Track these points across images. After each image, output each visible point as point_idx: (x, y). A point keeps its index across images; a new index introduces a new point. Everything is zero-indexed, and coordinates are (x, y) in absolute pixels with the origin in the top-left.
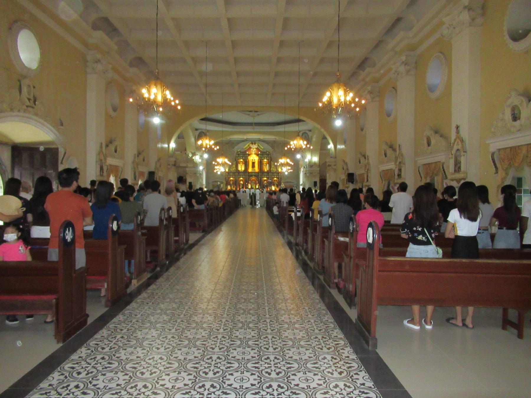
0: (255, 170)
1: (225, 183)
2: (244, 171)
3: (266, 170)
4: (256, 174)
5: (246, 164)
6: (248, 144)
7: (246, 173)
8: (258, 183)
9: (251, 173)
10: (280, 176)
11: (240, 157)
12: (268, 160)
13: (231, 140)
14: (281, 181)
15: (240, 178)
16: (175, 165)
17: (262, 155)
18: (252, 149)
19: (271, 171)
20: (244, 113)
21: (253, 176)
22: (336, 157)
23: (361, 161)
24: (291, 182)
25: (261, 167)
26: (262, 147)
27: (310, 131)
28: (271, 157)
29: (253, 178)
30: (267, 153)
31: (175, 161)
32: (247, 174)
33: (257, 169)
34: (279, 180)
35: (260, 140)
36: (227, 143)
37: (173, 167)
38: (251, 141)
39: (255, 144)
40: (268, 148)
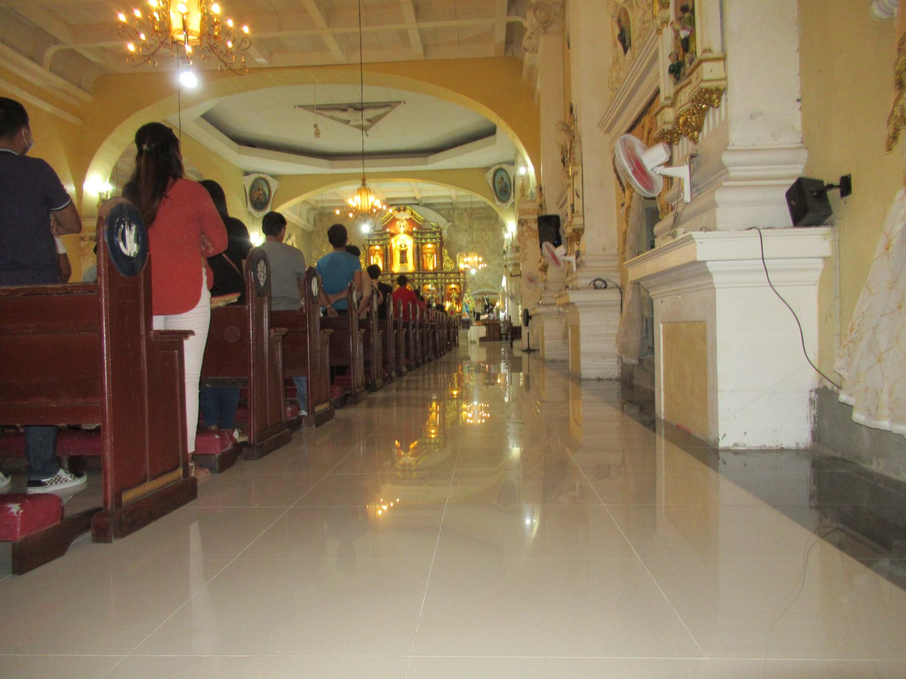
3: (431, 268)
7: (386, 274)
10: (462, 280)
12: (435, 244)
17: (422, 234)
18: (398, 223)
19: (442, 269)
20: (331, 117)
25: (418, 260)
28: (441, 239)
30: (434, 228)
32: (389, 276)
33: (410, 267)
34: (460, 289)
39: (405, 210)
40: (435, 219)
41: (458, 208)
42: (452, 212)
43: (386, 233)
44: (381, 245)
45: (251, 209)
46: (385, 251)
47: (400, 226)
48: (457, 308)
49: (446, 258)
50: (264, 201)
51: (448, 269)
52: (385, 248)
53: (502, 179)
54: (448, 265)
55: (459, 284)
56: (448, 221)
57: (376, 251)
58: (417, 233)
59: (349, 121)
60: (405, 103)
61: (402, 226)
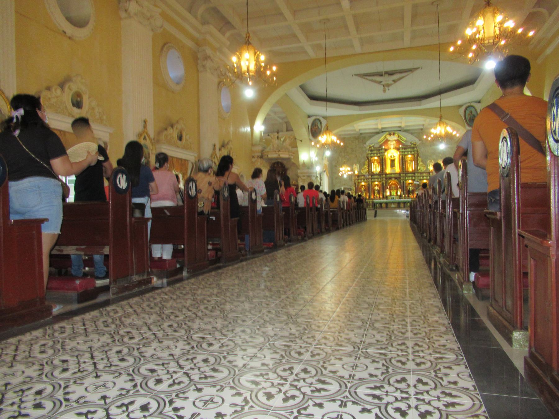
0: (395, 170)
1: (355, 190)
2: (380, 172)
3: (411, 170)
4: (397, 175)
5: (382, 162)
6: (384, 135)
7: (382, 175)
8: (400, 188)
11: (374, 154)
12: (414, 155)
13: (361, 132)
15: (375, 181)
16: (262, 157)
17: (405, 149)
18: (389, 142)
19: (418, 170)
20: (372, 81)
21: (393, 179)
25: (403, 165)
26: (404, 138)
28: (417, 151)
29: (393, 181)
31: (262, 151)
32: (384, 176)
33: (397, 169)
35: (401, 130)
36: (357, 138)
37: (259, 160)
39: (394, 134)
43: (382, 149)
44: (379, 157)
49: (420, 163)
53: (471, 112)
54: (421, 168)
56: (419, 140)
57: (375, 160)
58: (402, 148)
59: (381, 82)
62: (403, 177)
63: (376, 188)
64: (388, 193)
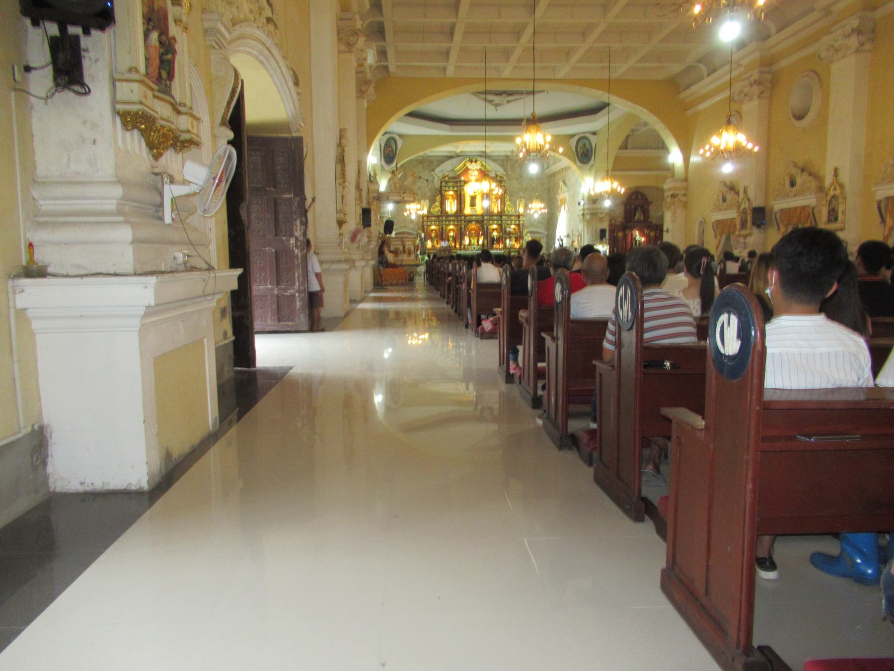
0: (476, 211)
2: (456, 212)
3: (496, 211)
4: (479, 217)
6: (464, 162)
7: (461, 216)
8: (482, 234)
9: (468, 216)
10: (521, 222)
11: (449, 187)
14: (523, 230)
15: (450, 225)
18: (470, 172)
21: (474, 223)
22: (686, 180)
23: (799, 181)
24: (537, 233)
27: (594, 133)
28: (505, 186)
29: (473, 226)
32: (463, 218)
35: (485, 155)
38: (466, 156)
39: (476, 161)
41: (511, 160)
42: (505, 163)
43: (460, 181)
44: (456, 192)
45: (383, 163)
46: (459, 196)
47: (472, 175)
48: (516, 245)
49: (508, 203)
50: (392, 156)
51: (509, 212)
52: (459, 193)
53: (585, 145)
54: (509, 209)
55: (518, 225)
57: (449, 195)
60: (548, 92)
61: (473, 175)
62: (487, 220)
63: (451, 234)
64: (466, 241)
